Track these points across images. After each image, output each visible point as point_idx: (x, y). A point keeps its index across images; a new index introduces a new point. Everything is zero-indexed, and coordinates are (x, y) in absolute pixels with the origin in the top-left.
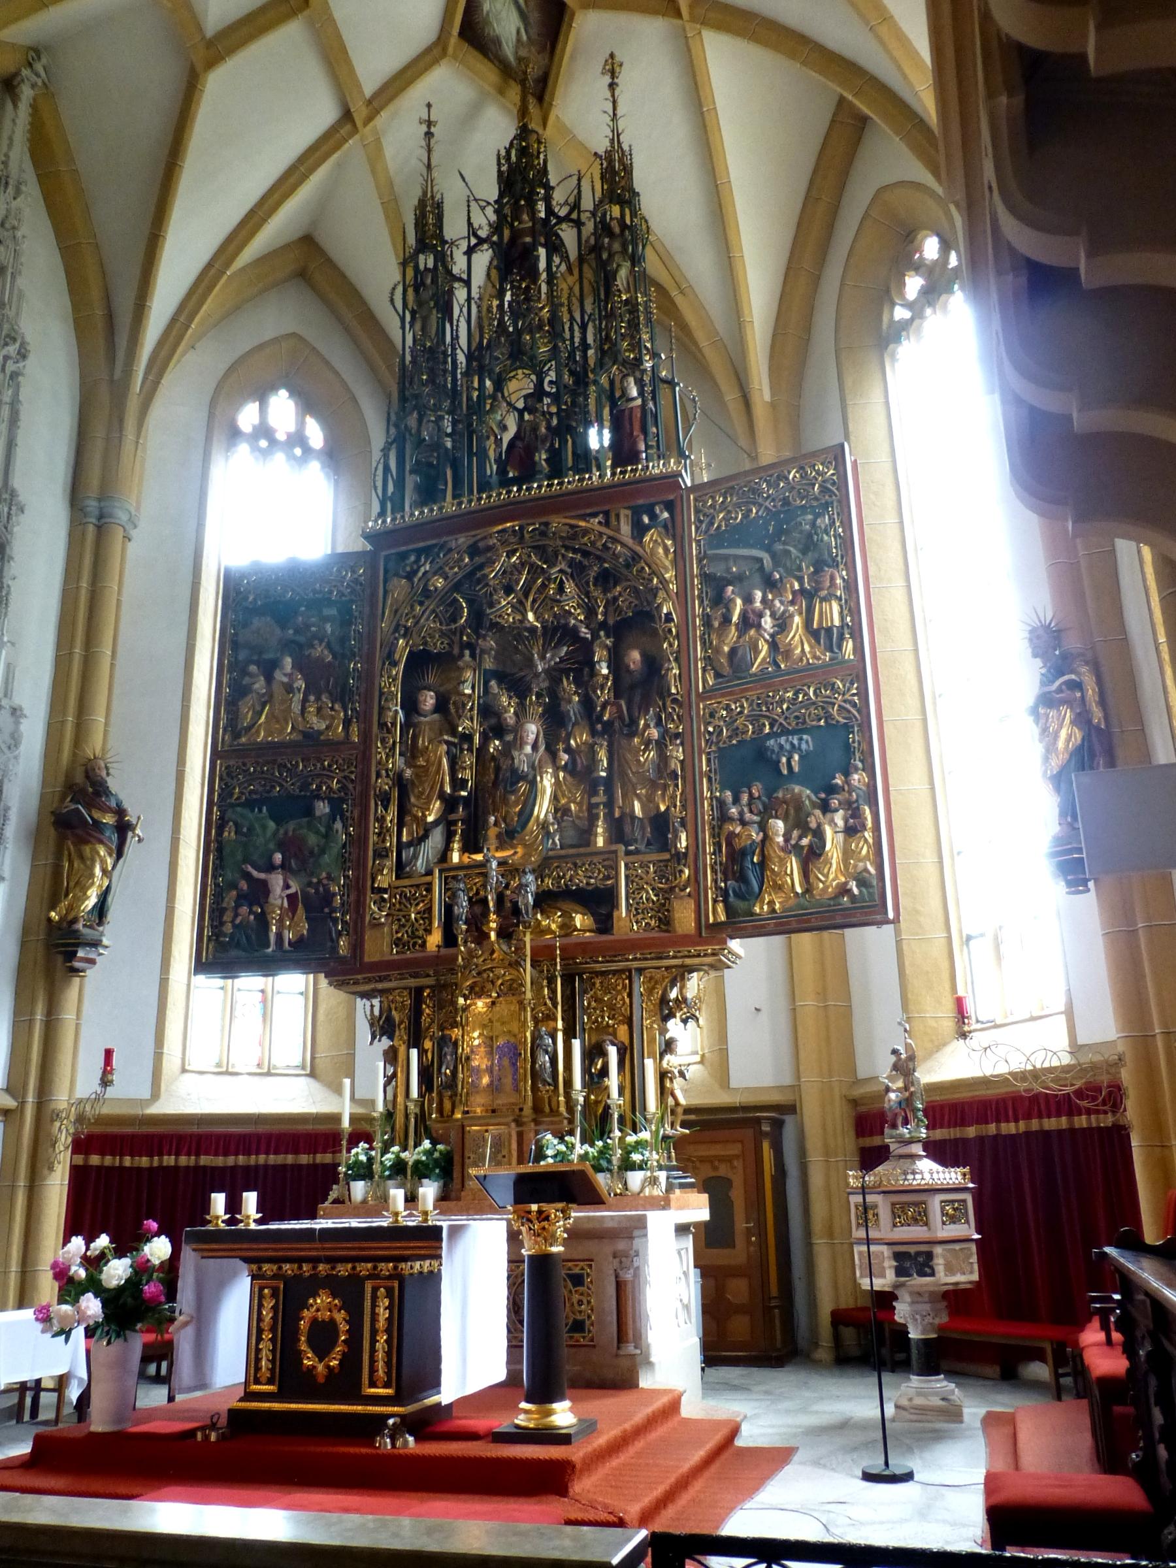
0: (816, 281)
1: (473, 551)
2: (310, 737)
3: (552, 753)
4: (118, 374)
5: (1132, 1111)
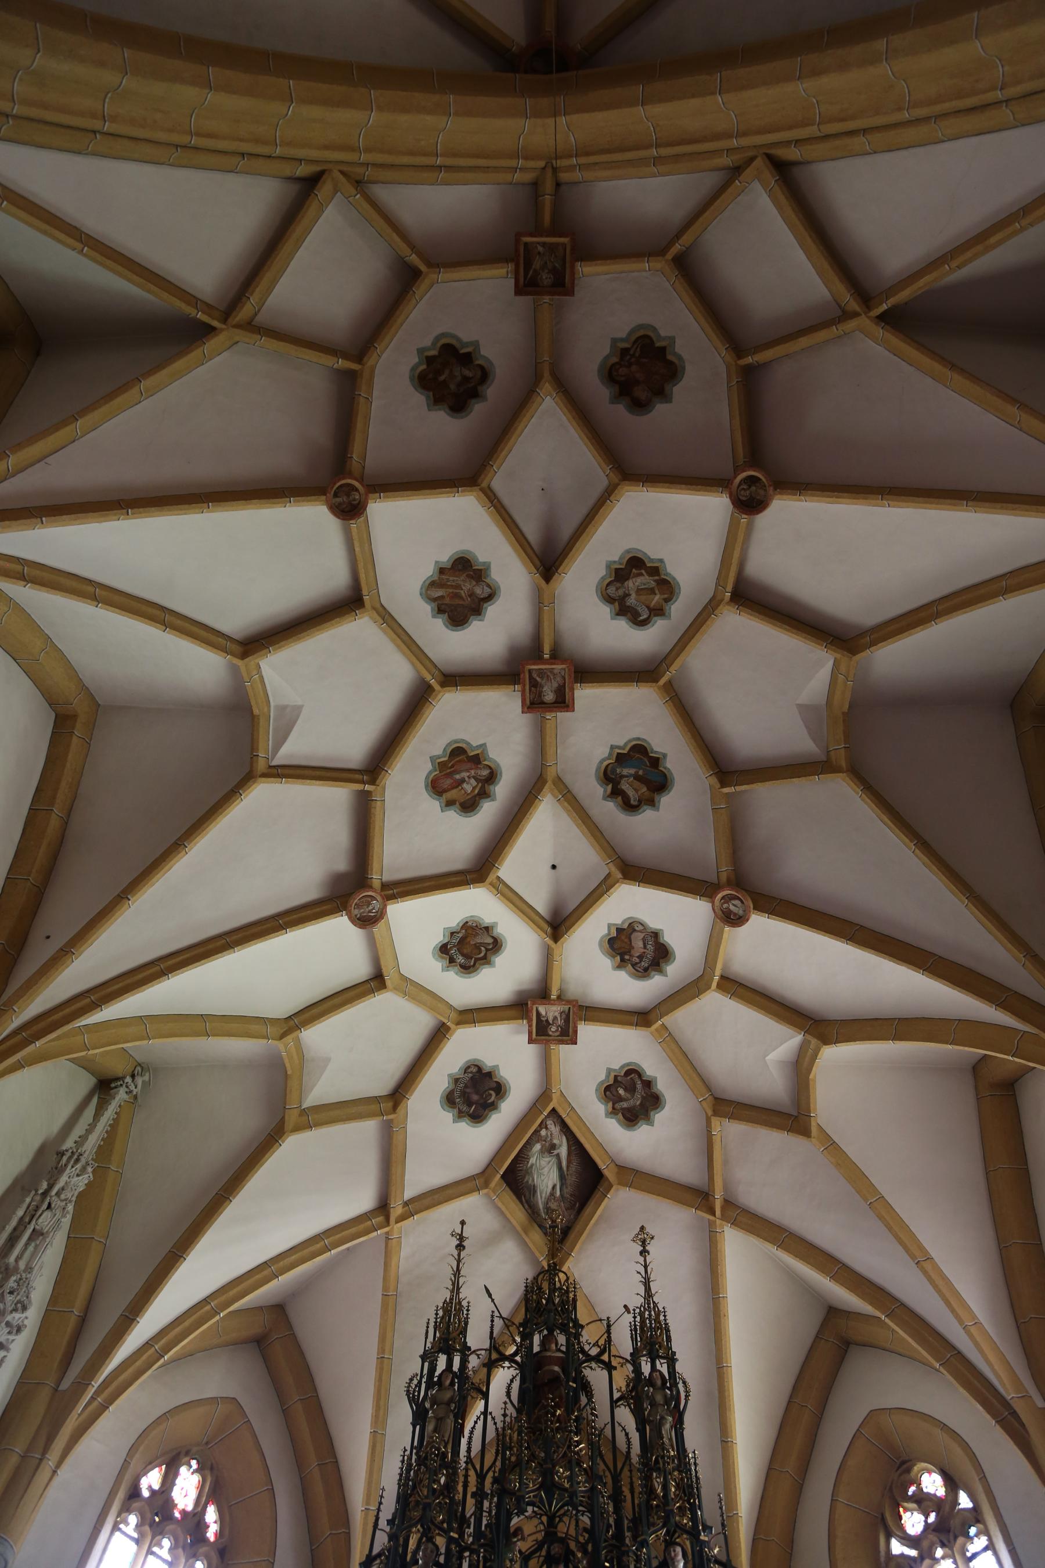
4: (65, 1385)
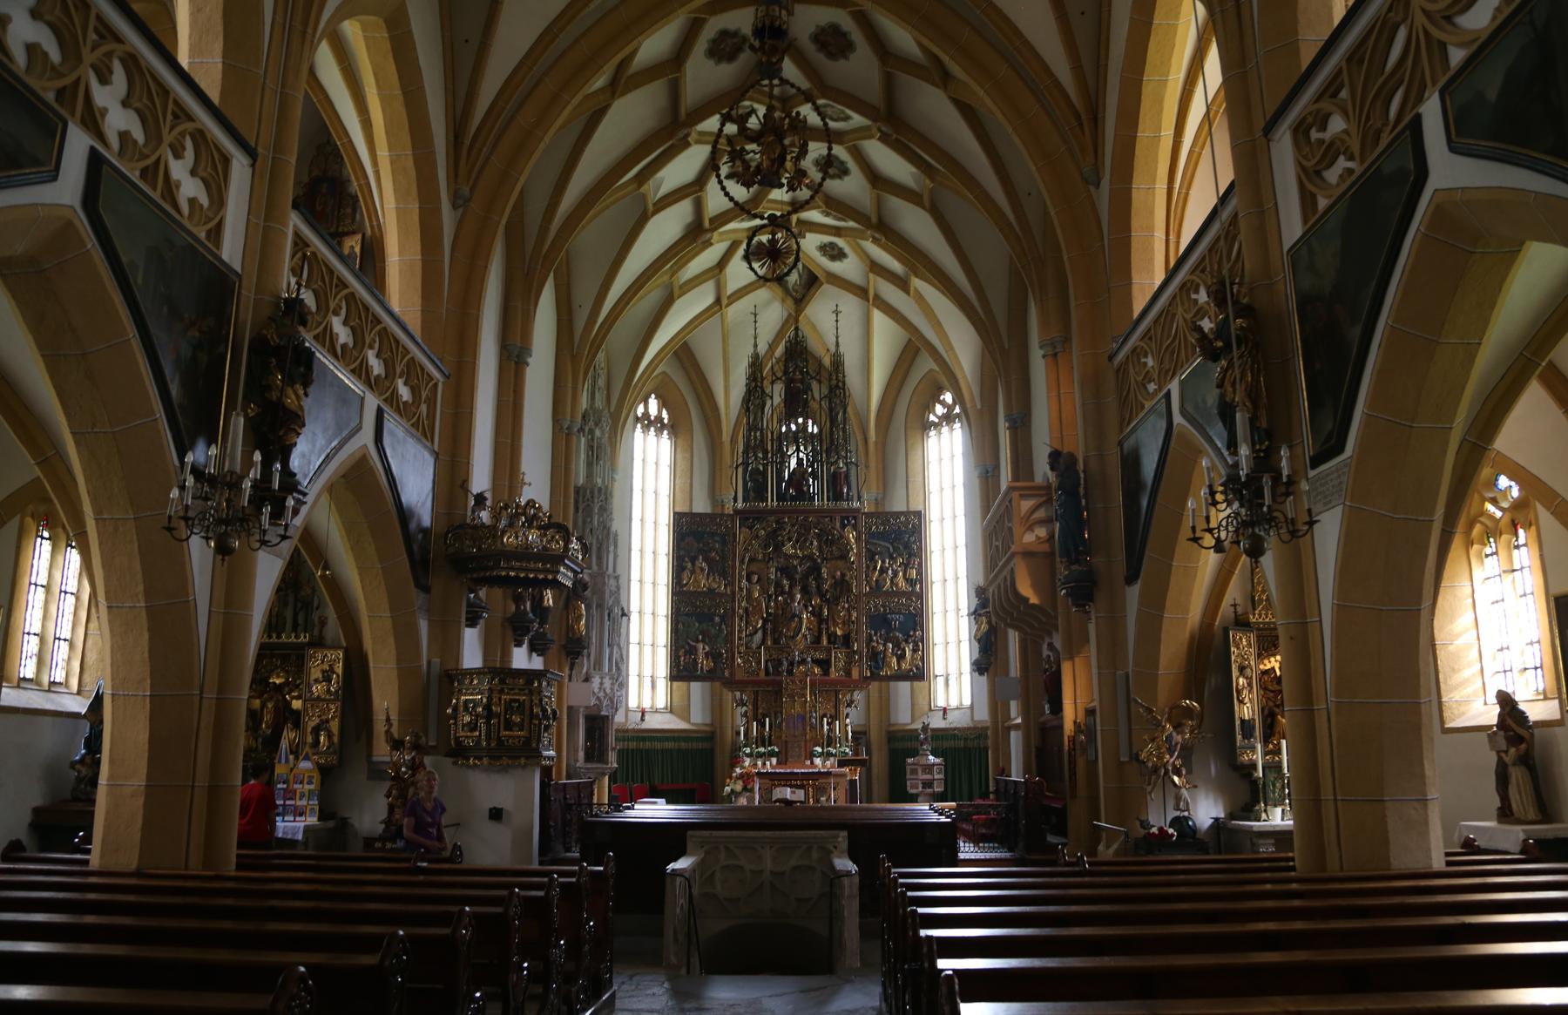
0: (899, 391)
1: (777, 522)
2: (711, 591)
3: (806, 606)
5: (989, 742)
